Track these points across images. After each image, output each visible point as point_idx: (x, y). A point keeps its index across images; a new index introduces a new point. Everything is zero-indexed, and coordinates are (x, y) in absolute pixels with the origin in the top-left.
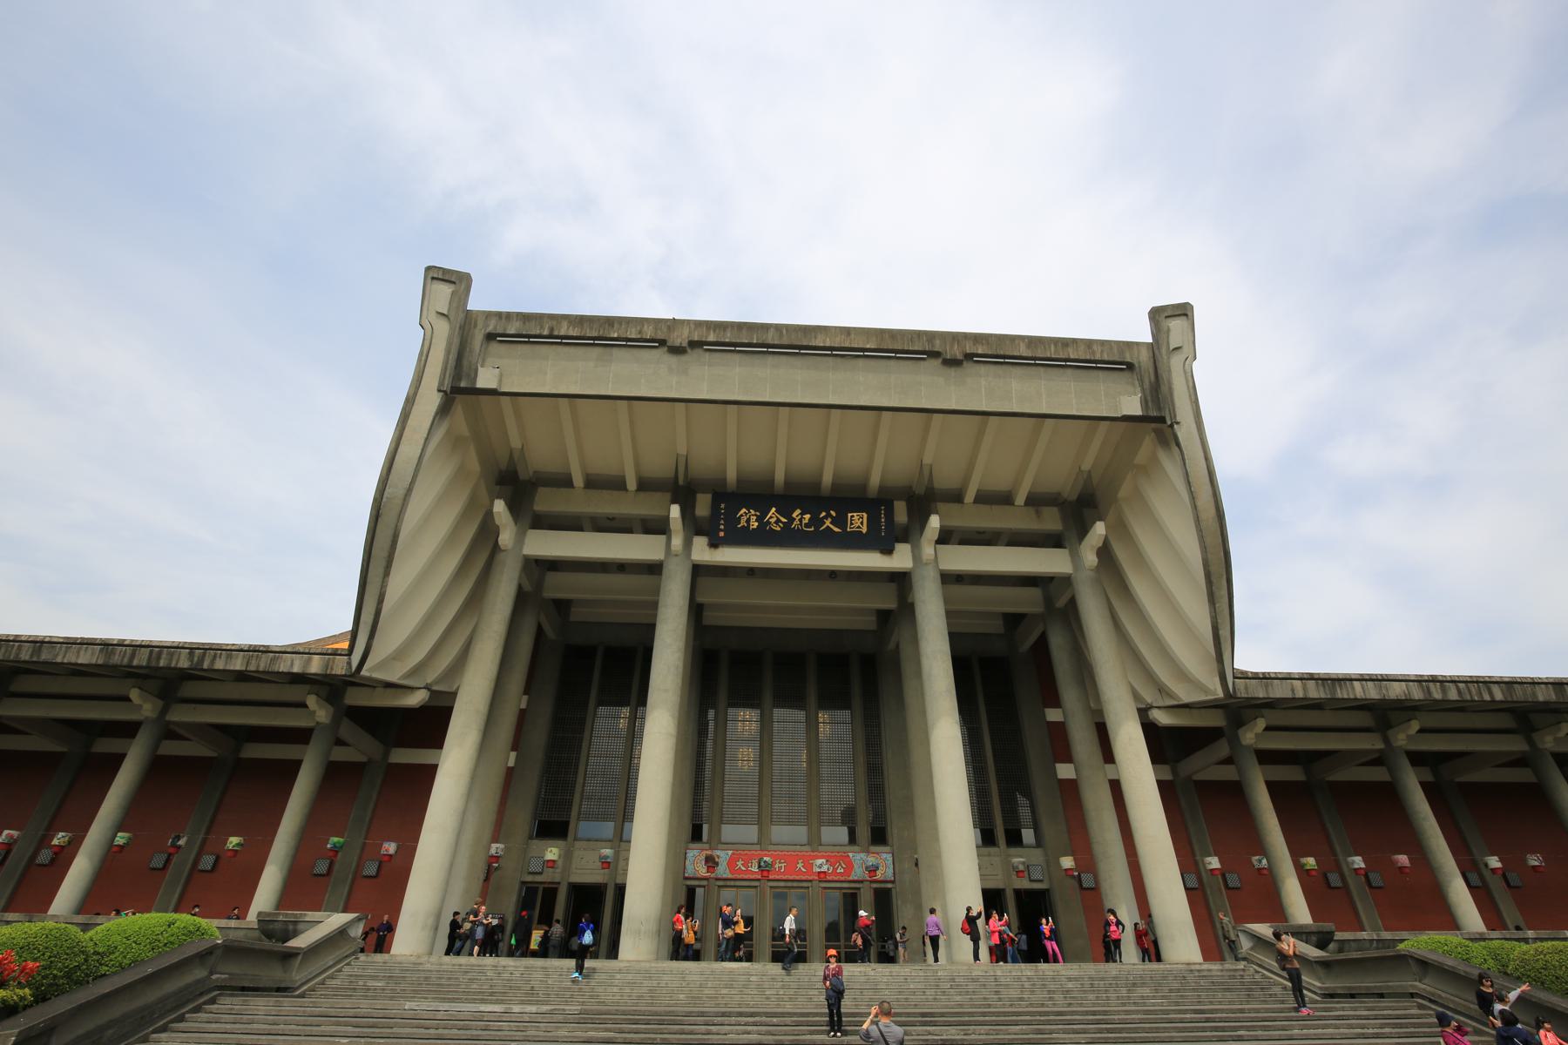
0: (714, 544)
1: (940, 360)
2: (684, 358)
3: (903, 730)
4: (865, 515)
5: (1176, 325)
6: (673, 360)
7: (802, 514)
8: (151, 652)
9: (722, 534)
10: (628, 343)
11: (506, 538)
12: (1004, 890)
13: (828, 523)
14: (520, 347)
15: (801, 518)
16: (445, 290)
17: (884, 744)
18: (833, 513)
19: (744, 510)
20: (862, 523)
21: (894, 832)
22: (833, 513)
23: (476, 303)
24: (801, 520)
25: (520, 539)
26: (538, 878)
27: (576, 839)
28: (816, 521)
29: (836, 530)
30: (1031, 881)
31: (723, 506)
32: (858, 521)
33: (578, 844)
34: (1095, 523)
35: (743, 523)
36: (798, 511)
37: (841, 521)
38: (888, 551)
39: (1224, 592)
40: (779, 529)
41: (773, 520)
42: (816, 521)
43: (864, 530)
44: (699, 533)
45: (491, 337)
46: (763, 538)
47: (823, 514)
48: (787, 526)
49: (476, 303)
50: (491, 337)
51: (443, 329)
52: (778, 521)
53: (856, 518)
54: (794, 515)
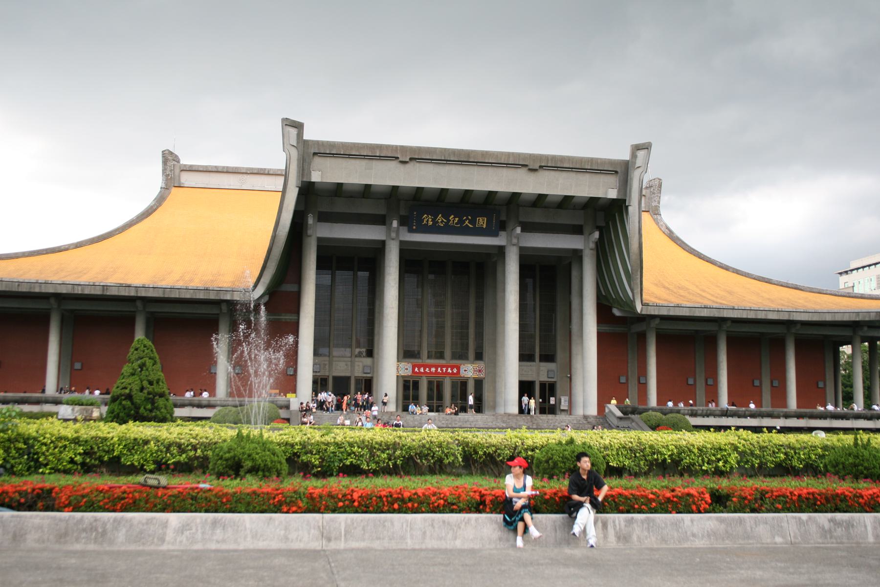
0: (411, 231)
1: (527, 168)
2: (407, 166)
3: (495, 305)
4: (485, 219)
5: (641, 154)
6: (402, 166)
7: (454, 218)
8: (164, 291)
9: (414, 227)
10: (381, 158)
12: (535, 381)
13: (467, 222)
14: (328, 159)
15: (454, 220)
16: (293, 132)
17: (485, 307)
18: (470, 217)
19: (425, 215)
20: (484, 223)
21: (486, 356)
22: (470, 217)
23: (307, 136)
24: (453, 221)
27: (333, 357)
28: (461, 222)
29: (471, 226)
30: (548, 377)
31: (415, 213)
32: (482, 222)
33: (335, 359)
34: (594, 232)
35: (425, 222)
36: (452, 216)
37: (473, 222)
38: (496, 235)
39: (639, 276)
40: (442, 225)
41: (440, 221)
42: (461, 222)
43: (484, 226)
45: (315, 154)
46: (435, 229)
47: (465, 218)
48: (447, 223)
49: (305, 138)
50: (315, 154)
51: (294, 153)
52: (442, 221)
53: (481, 220)
54: (450, 218)
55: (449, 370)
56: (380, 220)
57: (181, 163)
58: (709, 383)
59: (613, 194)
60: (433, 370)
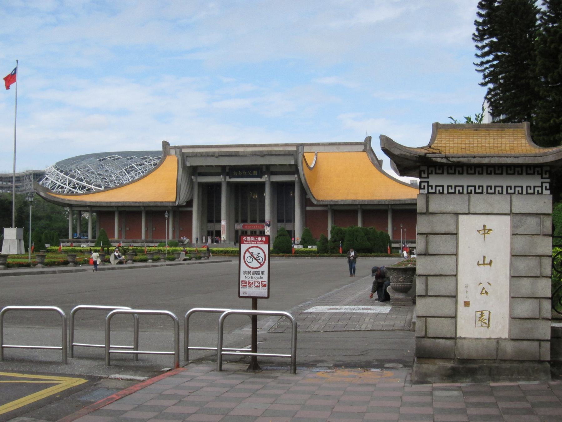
0: (230, 178)
11: (194, 180)
13: (250, 173)
15: (245, 173)
25: (196, 179)
26: (210, 230)
32: (255, 173)
35: (234, 174)
37: (252, 173)
38: (261, 177)
44: (227, 175)
45: (187, 157)
46: (238, 177)
48: (242, 175)
50: (187, 157)
51: (180, 157)
55: (254, 227)
56: (218, 174)
57: (170, 145)
58: (394, 229)
59: (292, 162)
60: (254, 227)
